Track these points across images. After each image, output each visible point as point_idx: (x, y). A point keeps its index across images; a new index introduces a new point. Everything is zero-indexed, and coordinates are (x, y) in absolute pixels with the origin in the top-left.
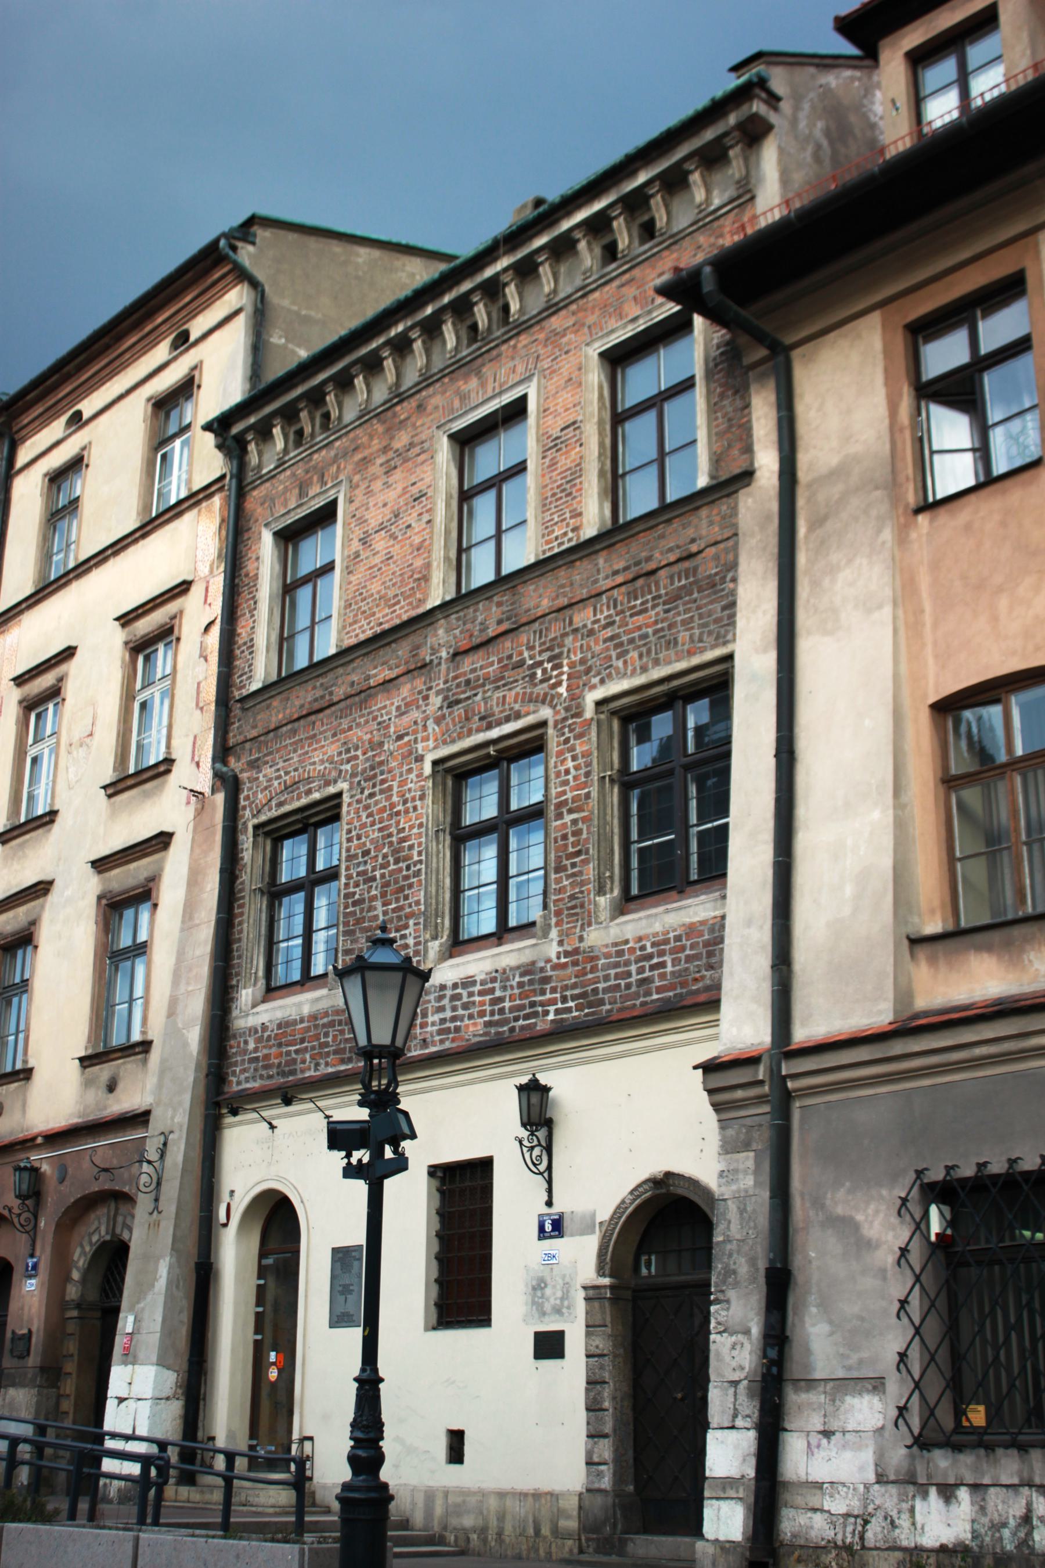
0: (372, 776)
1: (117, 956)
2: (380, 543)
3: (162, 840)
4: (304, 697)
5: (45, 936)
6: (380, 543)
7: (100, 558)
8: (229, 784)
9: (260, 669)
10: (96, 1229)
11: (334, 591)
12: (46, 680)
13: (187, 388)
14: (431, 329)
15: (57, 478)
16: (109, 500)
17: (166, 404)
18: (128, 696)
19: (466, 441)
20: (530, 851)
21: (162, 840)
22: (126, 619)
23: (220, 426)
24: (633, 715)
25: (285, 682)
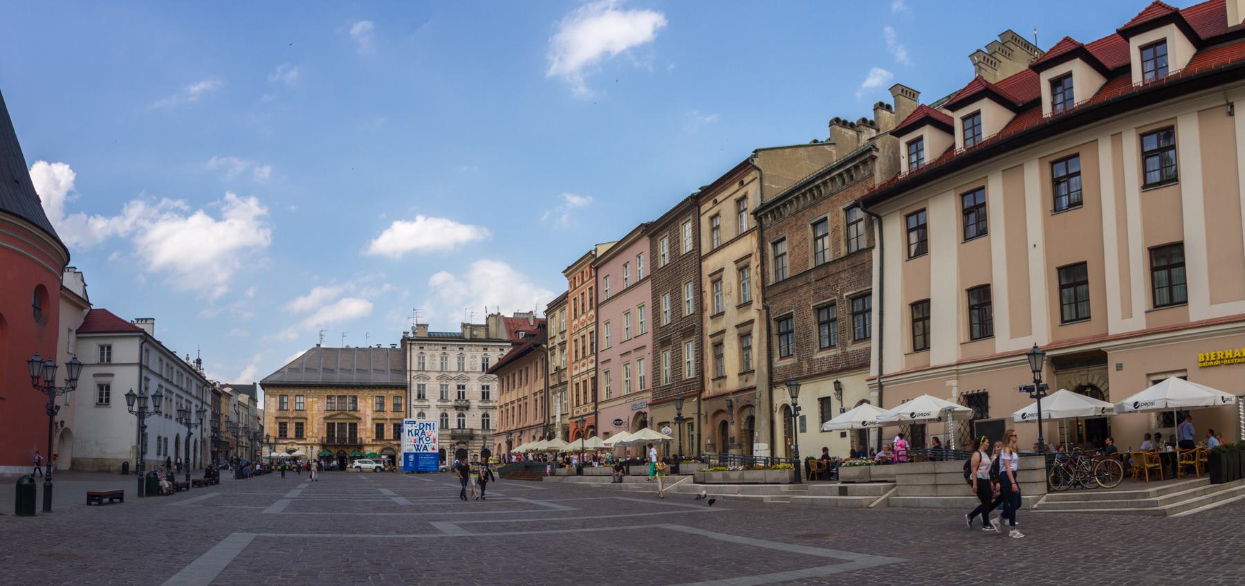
0: (799, 308)
1: (745, 349)
4: (782, 288)
5: (725, 343)
7: (727, 244)
8: (766, 308)
9: (772, 279)
10: (747, 413)
12: (717, 276)
13: (745, 197)
14: (804, 195)
15: (712, 218)
16: (728, 229)
17: (739, 201)
18: (739, 282)
19: (815, 225)
20: (835, 328)
21: (752, 321)
22: (736, 262)
23: (755, 213)
24: (853, 299)
25: (777, 284)
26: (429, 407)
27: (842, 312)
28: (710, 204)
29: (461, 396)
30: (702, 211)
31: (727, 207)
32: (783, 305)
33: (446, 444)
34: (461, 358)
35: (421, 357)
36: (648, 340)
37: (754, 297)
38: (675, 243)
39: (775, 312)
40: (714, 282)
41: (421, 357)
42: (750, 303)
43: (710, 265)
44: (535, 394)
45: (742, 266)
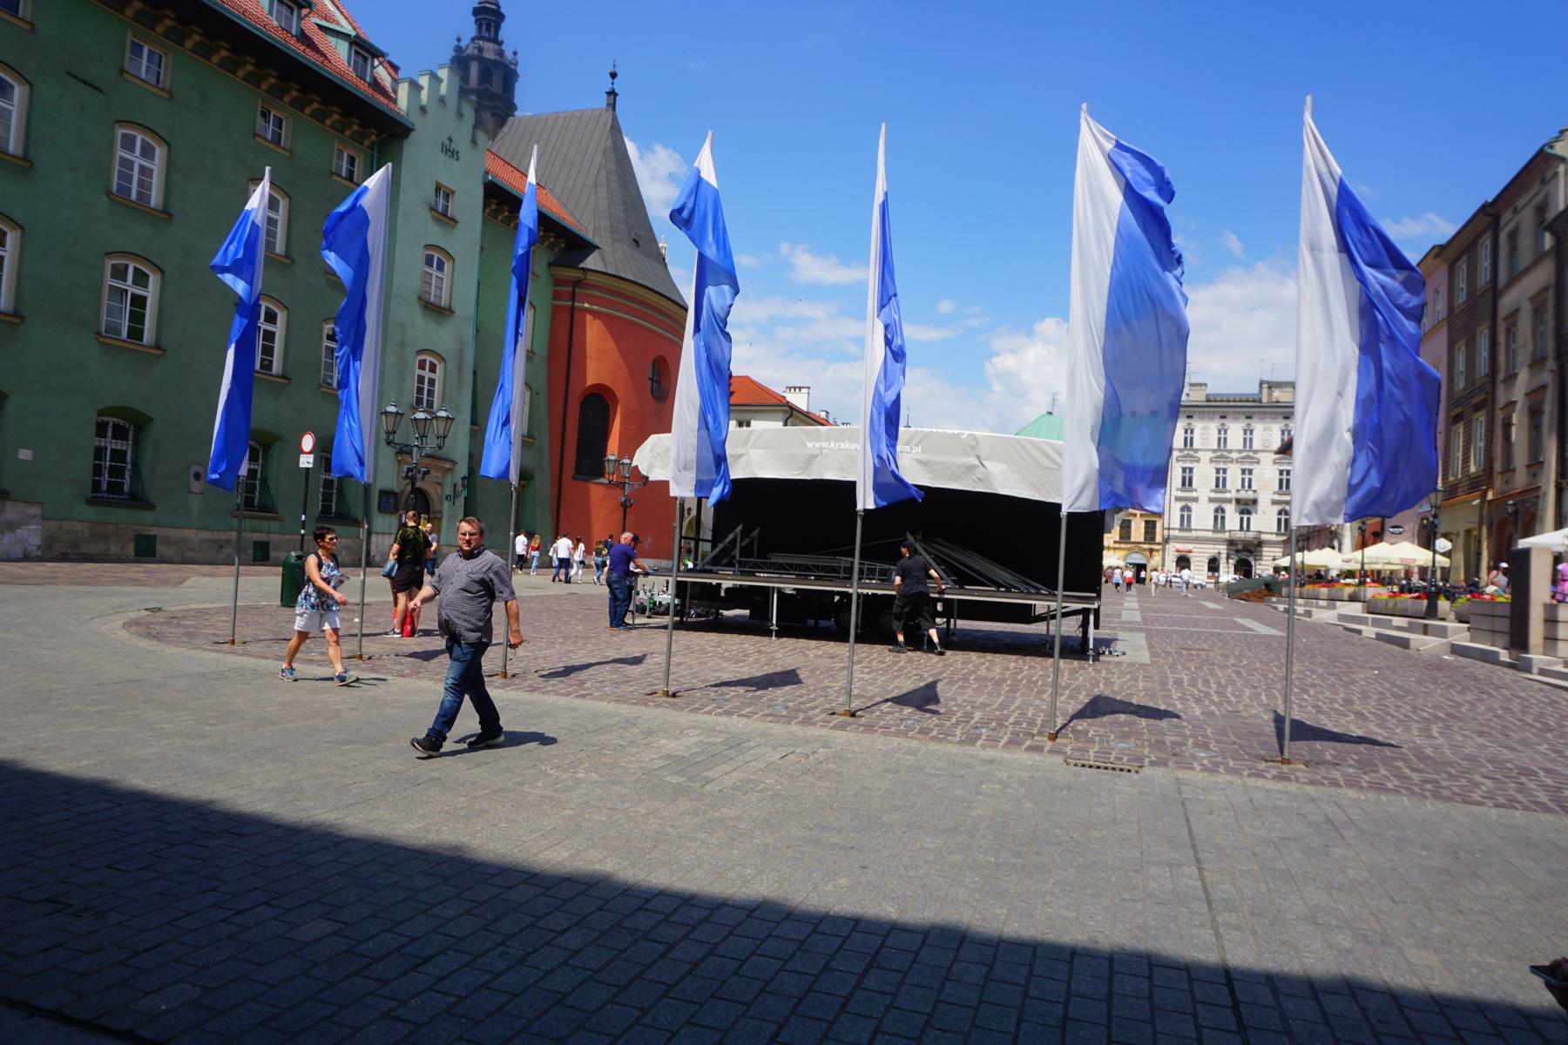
26: (1196, 500)
33: (1223, 549)
34: (1248, 431)
35: (1189, 431)
41: (1189, 431)
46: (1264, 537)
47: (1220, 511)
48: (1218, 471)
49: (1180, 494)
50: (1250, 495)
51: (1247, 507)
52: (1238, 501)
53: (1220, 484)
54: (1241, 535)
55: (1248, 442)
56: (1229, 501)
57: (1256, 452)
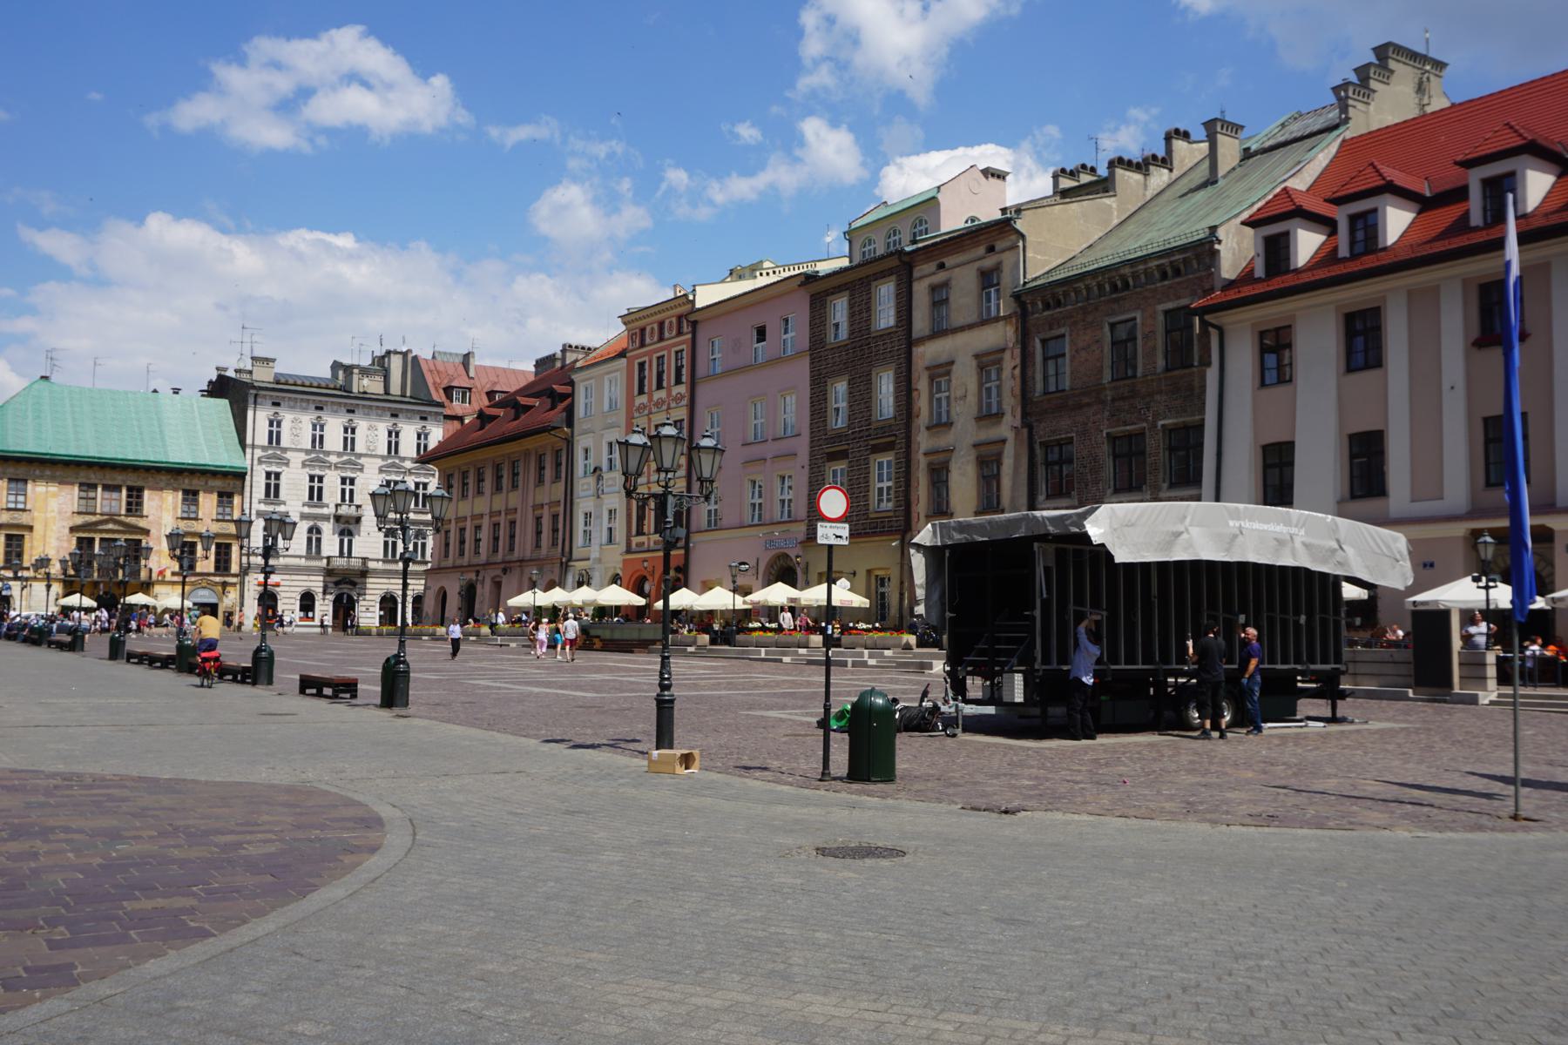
2: (1083, 354)
3: (1004, 441)
6: (1083, 354)
11: (1067, 365)
15: (934, 289)
18: (981, 385)
21: (1004, 441)
22: (977, 356)
24: (1170, 431)
27: (1156, 447)
28: (932, 266)
29: (347, 496)
30: (916, 274)
31: (964, 278)
32: (1063, 426)
33: (316, 584)
34: (350, 429)
35: (275, 422)
36: (803, 446)
37: (1007, 407)
38: (861, 312)
39: (1043, 432)
40: (932, 379)
41: (275, 422)
42: (1000, 415)
43: (927, 353)
44: (535, 507)
45: (987, 362)
46: (371, 565)
47: (314, 531)
48: (312, 478)
49: (263, 507)
50: (352, 511)
51: (347, 526)
52: (338, 518)
53: (316, 495)
54: (340, 563)
55: (349, 443)
56: (326, 518)
57: (360, 456)
